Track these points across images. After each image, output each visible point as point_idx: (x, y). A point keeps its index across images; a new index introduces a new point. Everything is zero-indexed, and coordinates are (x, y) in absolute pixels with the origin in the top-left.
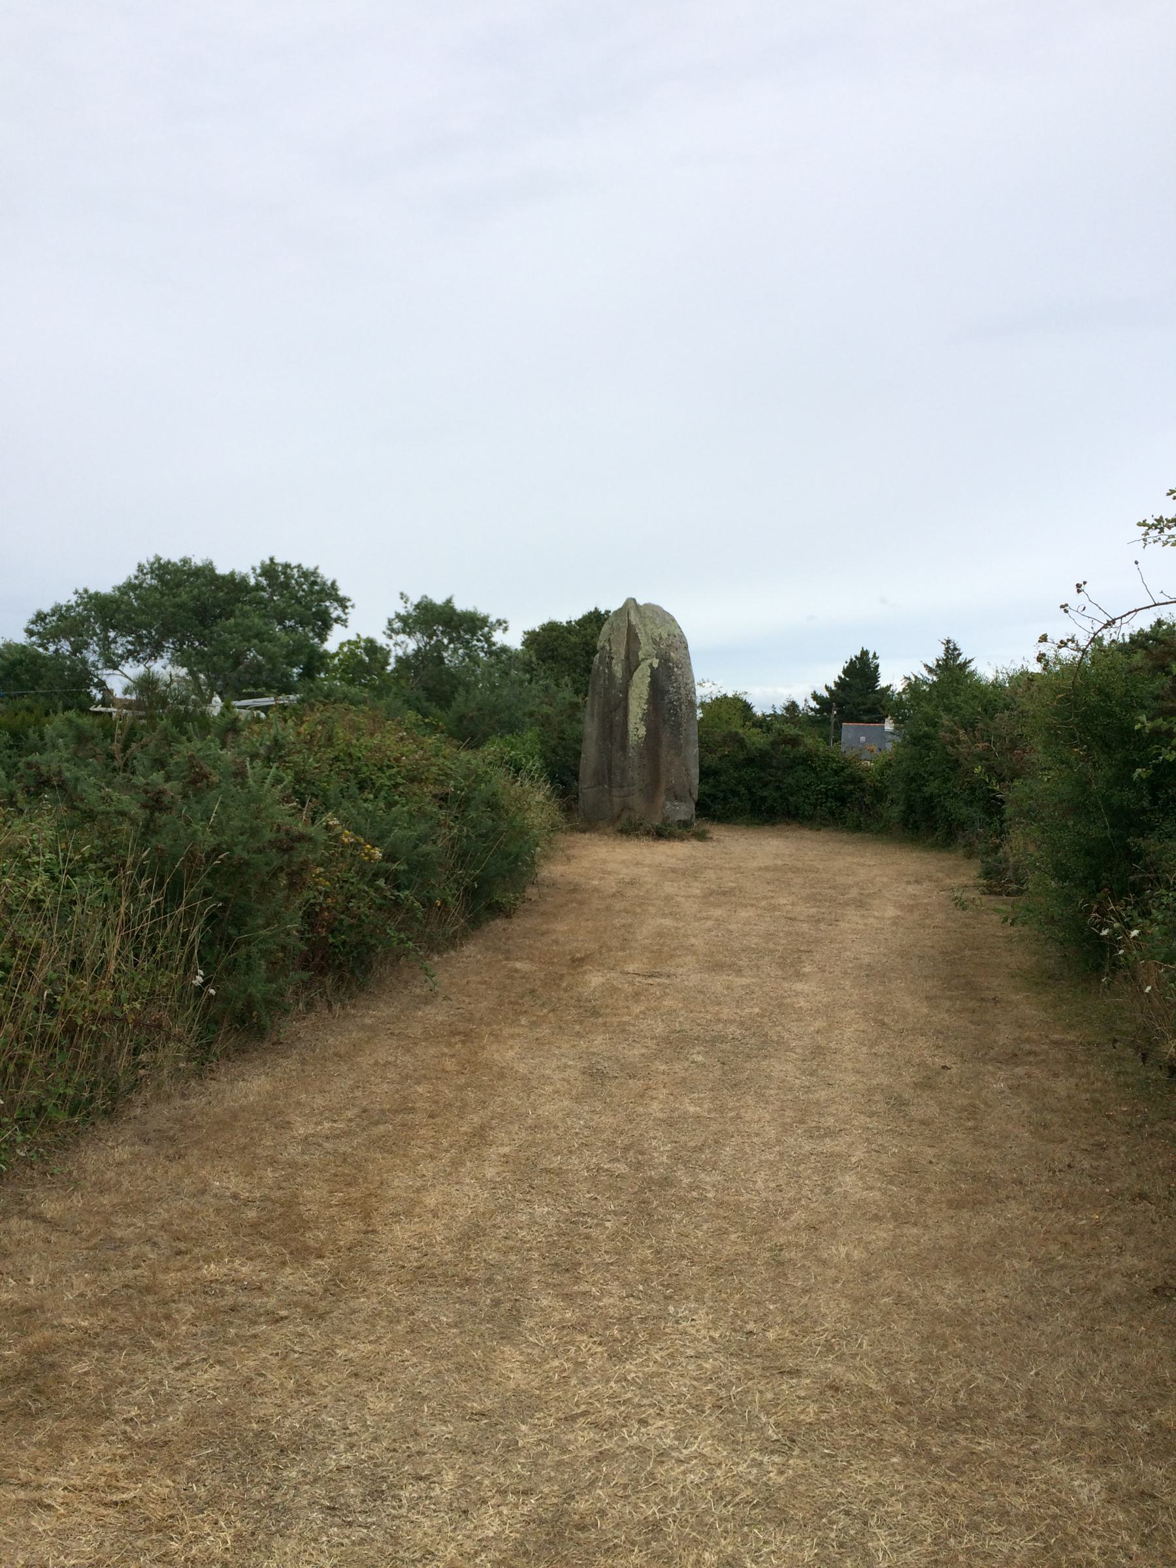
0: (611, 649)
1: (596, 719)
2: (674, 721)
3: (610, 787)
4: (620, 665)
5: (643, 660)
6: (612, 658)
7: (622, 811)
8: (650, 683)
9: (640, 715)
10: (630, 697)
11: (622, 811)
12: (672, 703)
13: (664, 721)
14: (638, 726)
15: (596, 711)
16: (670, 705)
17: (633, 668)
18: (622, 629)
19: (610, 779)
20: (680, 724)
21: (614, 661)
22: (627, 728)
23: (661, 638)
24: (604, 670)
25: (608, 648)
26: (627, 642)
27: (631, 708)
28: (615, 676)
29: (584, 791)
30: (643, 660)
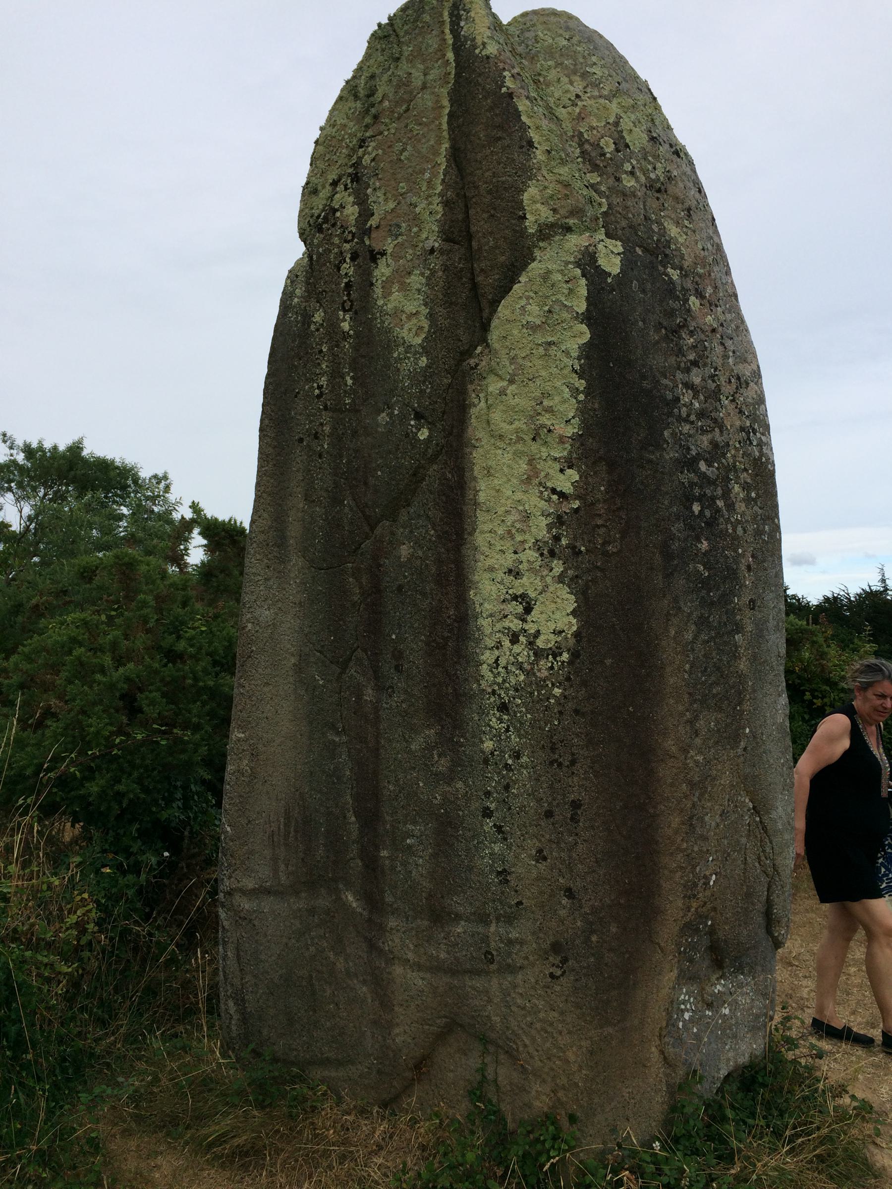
0: (366, 213)
1: (296, 562)
2: (707, 559)
3: (373, 901)
4: (416, 280)
5: (546, 232)
6: (374, 256)
7: (442, 1037)
8: (588, 351)
9: (540, 528)
10: (476, 430)
11: (442, 1037)
12: (691, 464)
13: (667, 555)
14: (527, 584)
15: (294, 530)
16: (686, 477)
17: (488, 282)
18: (426, 100)
19: (372, 865)
20: (732, 575)
21: (383, 270)
22: (462, 601)
23: (621, 145)
24: (332, 324)
25: (351, 212)
26: (456, 156)
27: (484, 490)
28: (391, 344)
29: (246, 905)
30: (546, 232)
